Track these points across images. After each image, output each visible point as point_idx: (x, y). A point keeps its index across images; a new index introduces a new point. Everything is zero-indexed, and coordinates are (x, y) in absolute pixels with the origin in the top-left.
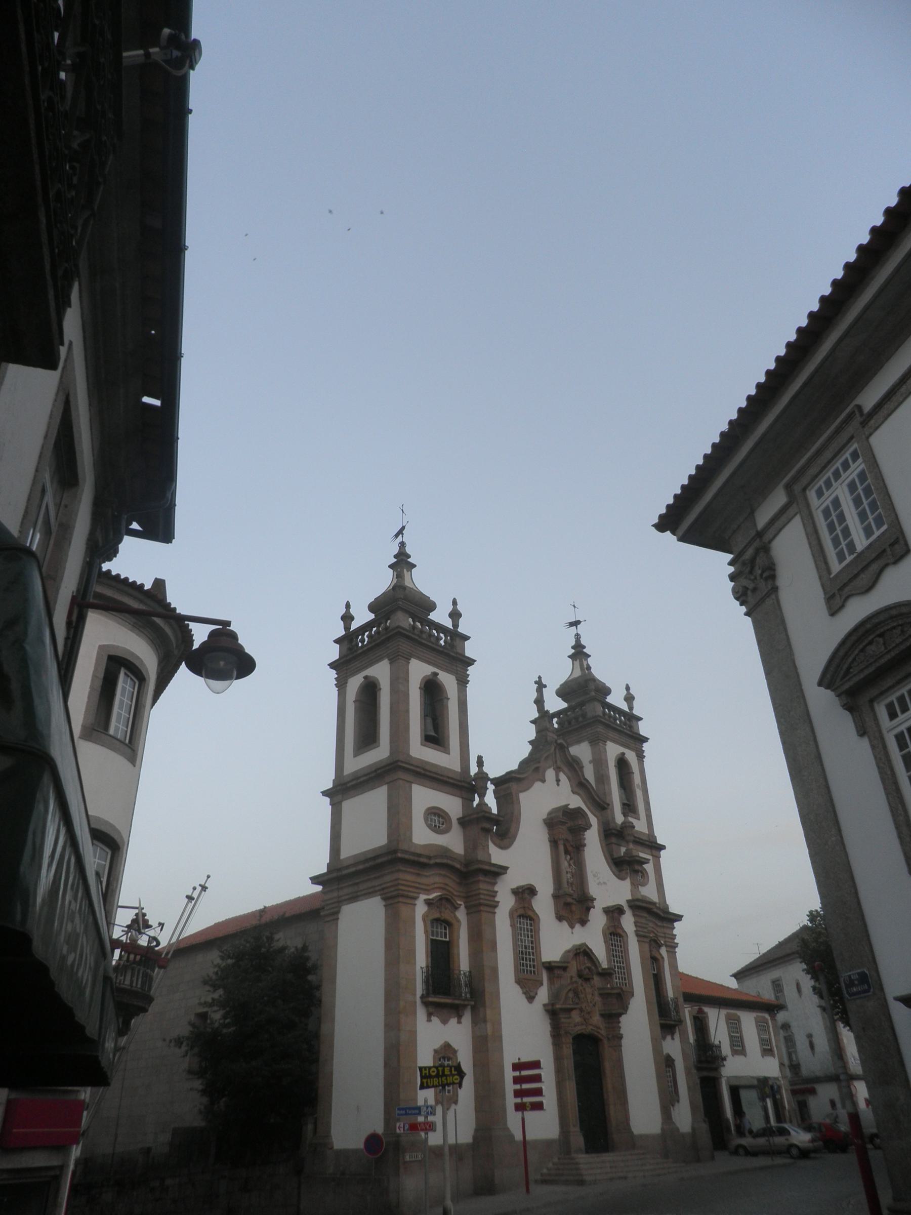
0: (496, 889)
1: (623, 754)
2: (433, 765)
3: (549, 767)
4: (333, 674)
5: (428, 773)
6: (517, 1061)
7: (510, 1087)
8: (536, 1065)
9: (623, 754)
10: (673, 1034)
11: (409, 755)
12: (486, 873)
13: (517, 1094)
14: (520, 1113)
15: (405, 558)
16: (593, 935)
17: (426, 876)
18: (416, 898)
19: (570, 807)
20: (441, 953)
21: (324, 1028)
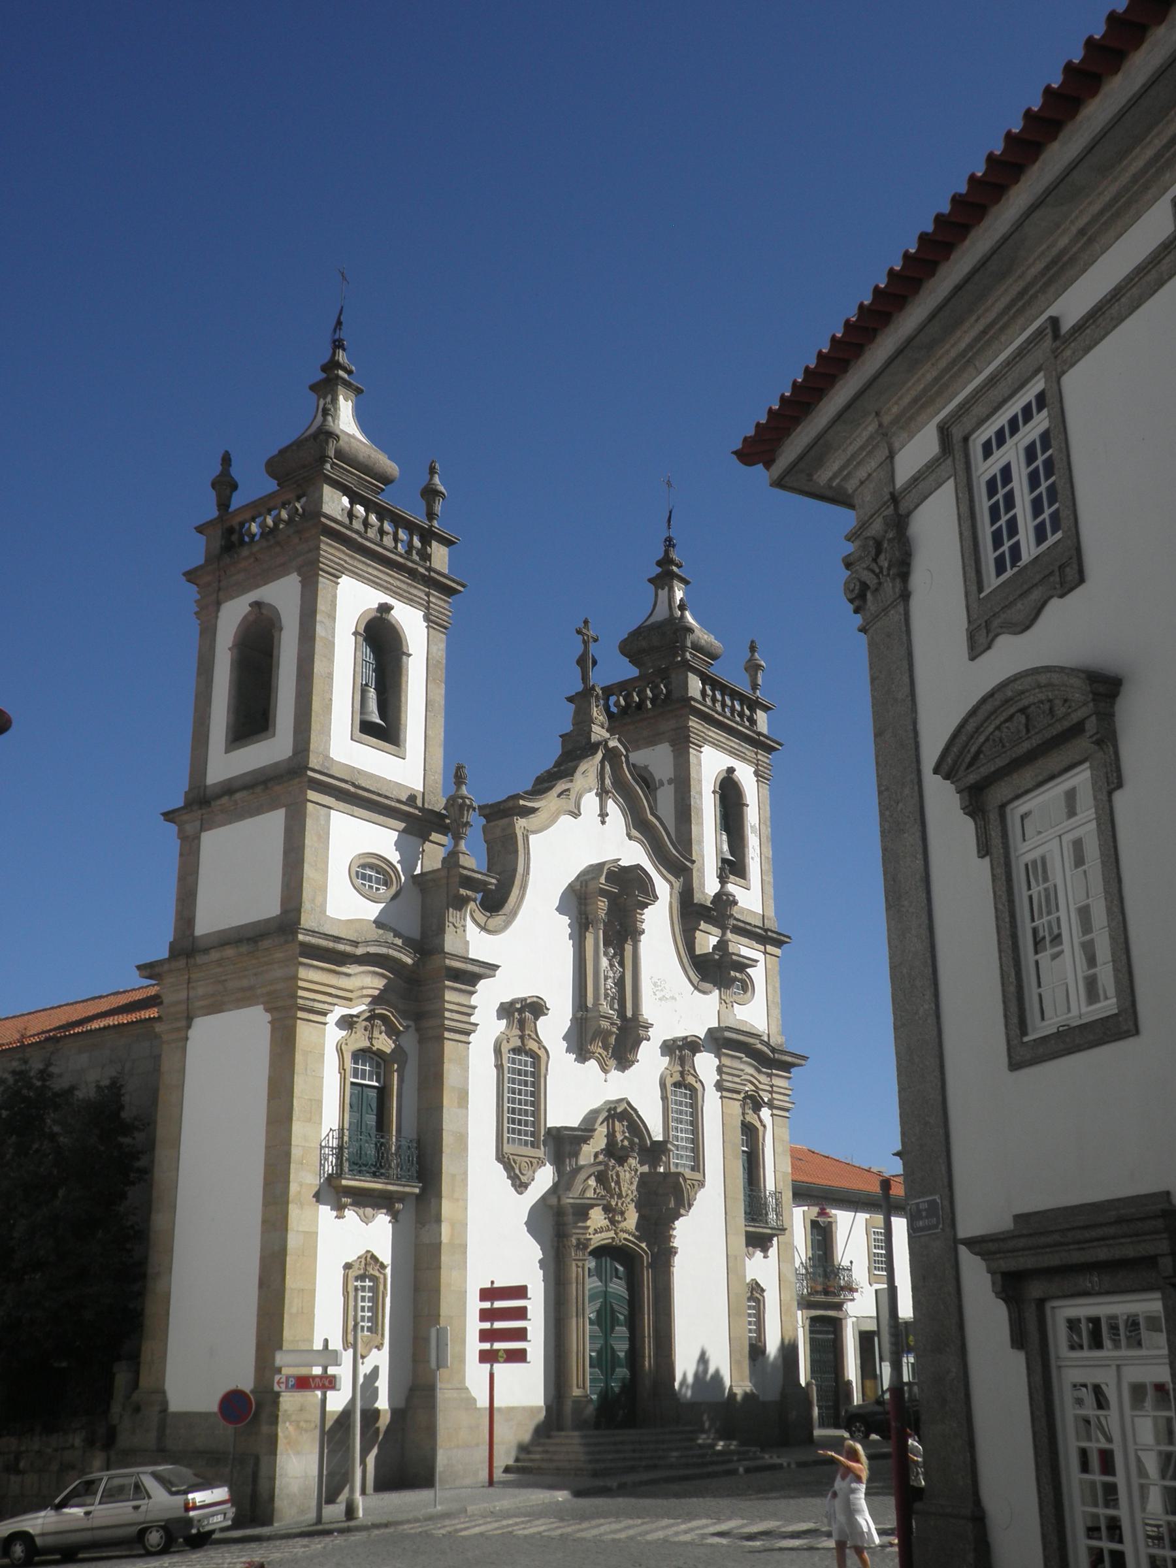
0: (474, 1000)
1: (731, 770)
2: (371, 776)
3: (590, 790)
4: (192, 591)
5: (361, 792)
6: (489, 1286)
7: (474, 1325)
8: (520, 1292)
9: (731, 770)
10: (765, 1250)
11: (327, 757)
13: (485, 1336)
14: (488, 1366)
15: (341, 373)
16: (641, 1085)
17: (348, 975)
19: (621, 863)
20: (371, 1107)
21: (158, 1220)
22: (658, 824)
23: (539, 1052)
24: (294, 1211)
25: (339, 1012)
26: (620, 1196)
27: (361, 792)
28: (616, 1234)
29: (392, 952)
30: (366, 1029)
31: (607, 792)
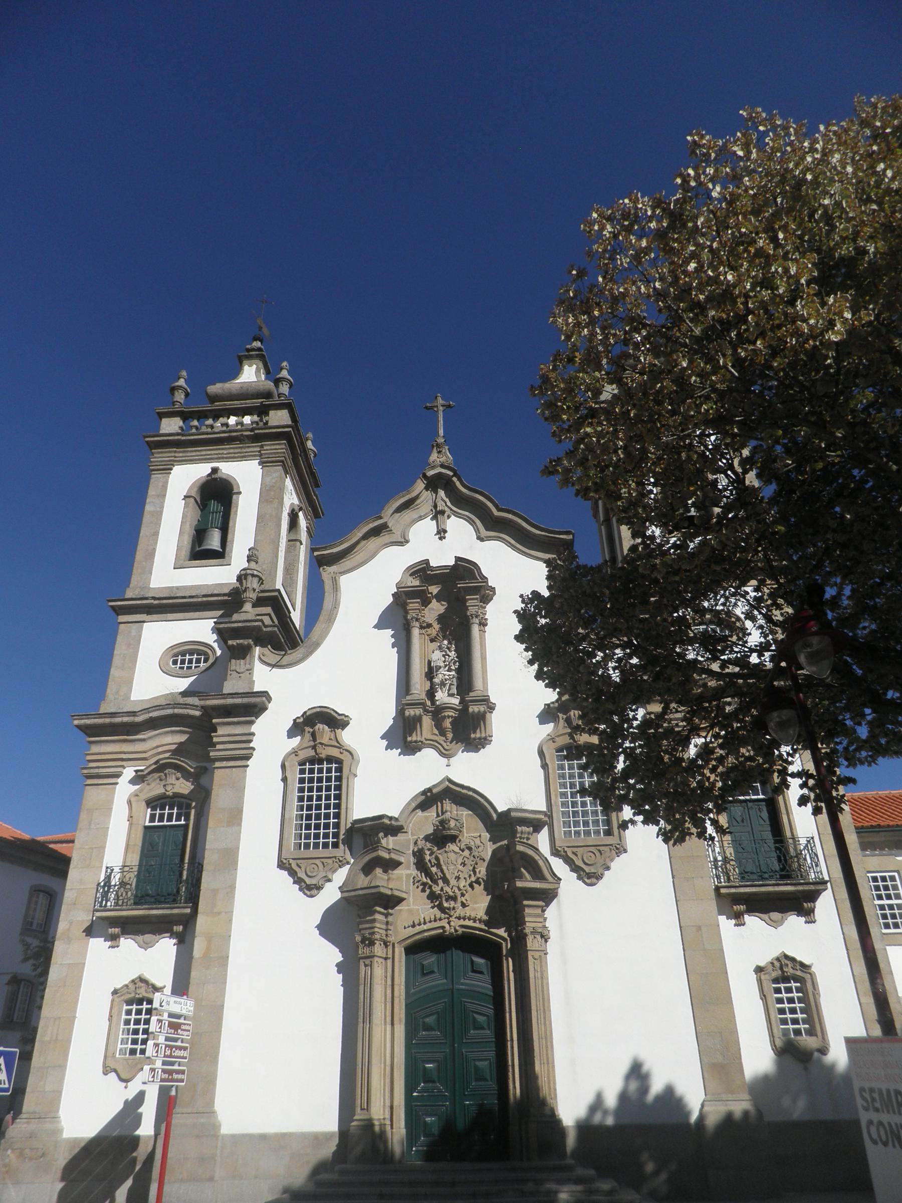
5: (165, 601)
10: (808, 914)
12: (228, 711)
17: (144, 740)
18: (118, 775)
22: (510, 516)
23: (341, 756)
24: (59, 948)
25: (129, 773)
26: (446, 881)
27: (165, 601)
28: (449, 923)
29: (176, 711)
30: (161, 780)
31: (442, 512)
